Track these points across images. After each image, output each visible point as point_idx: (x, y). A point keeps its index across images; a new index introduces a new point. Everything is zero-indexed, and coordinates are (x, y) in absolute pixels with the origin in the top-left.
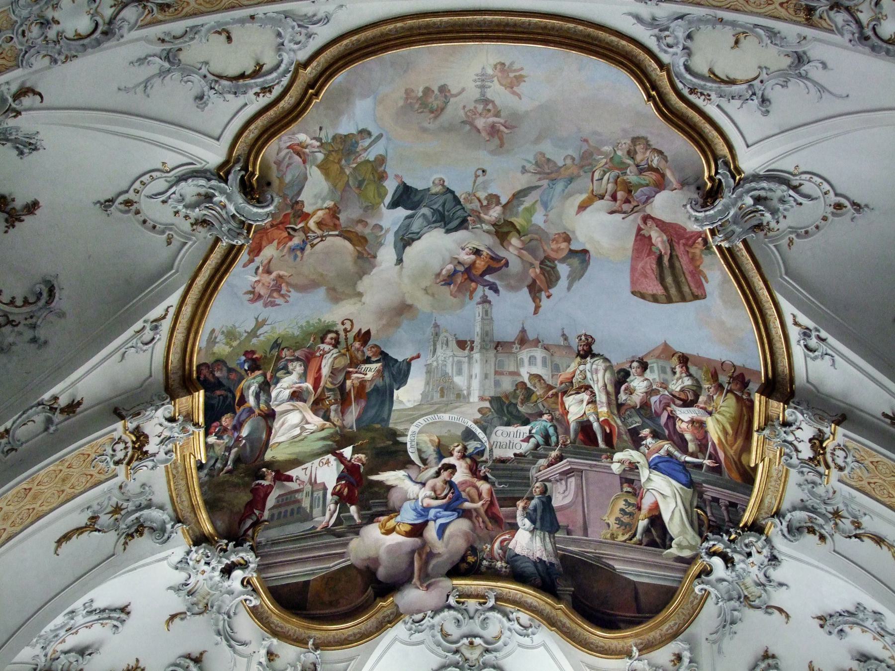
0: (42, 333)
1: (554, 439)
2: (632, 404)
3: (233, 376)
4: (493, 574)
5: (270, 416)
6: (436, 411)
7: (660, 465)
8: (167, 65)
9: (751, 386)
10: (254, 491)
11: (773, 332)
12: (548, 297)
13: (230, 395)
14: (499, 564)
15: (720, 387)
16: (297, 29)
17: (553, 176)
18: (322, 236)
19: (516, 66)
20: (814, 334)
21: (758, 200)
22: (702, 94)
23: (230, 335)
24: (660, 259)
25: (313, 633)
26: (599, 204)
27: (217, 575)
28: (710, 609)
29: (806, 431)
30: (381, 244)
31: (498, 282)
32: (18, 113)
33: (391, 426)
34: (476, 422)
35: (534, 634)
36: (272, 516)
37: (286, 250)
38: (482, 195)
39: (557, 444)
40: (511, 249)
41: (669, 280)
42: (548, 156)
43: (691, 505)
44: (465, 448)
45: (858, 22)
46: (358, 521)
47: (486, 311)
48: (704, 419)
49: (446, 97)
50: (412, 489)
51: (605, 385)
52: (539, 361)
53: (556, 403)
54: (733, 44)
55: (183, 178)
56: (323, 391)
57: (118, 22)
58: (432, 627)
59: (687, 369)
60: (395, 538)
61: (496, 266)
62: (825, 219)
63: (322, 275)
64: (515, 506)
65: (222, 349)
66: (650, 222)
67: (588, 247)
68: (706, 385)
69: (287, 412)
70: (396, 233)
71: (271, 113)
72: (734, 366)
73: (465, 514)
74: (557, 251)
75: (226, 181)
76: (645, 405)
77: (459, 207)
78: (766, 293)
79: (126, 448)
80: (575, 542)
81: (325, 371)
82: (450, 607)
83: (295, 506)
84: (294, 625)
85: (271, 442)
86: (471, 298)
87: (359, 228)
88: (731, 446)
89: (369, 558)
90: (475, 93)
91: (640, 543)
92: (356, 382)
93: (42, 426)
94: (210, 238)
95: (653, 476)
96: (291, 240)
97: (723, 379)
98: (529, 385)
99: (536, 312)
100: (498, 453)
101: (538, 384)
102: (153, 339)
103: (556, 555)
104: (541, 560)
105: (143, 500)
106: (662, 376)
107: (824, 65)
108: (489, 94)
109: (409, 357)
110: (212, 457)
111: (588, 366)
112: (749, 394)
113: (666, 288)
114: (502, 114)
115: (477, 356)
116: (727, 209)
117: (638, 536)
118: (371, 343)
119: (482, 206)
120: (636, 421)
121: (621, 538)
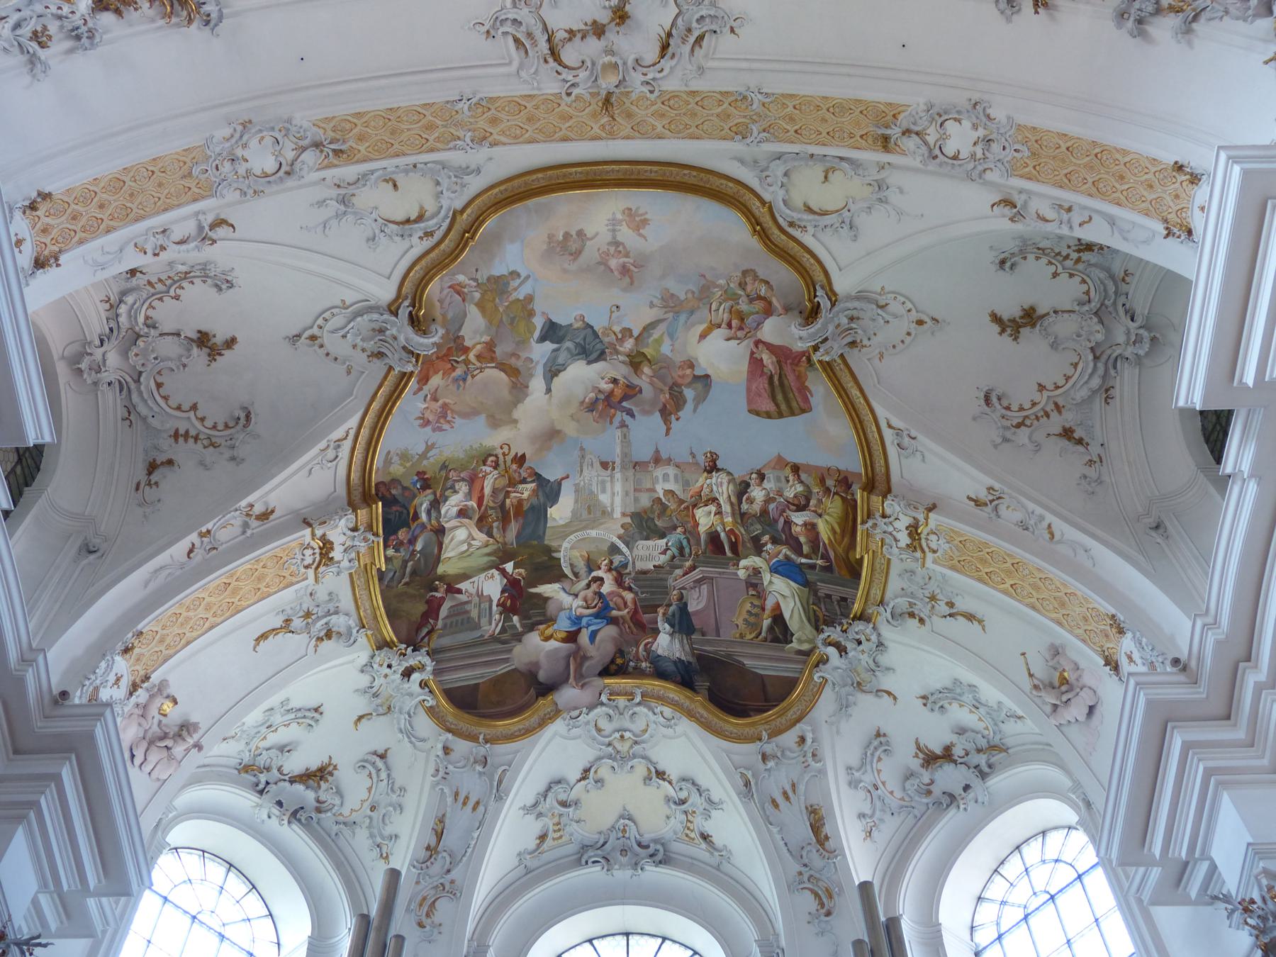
1: (687, 550)
2: (753, 513)
3: (406, 494)
4: (639, 673)
5: (440, 531)
6: (585, 528)
7: (780, 568)
8: (342, 208)
9: (853, 487)
10: (428, 602)
11: (870, 436)
12: (677, 419)
13: (405, 511)
14: (644, 665)
15: (827, 491)
16: (454, 179)
17: (677, 309)
18: (481, 368)
19: (641, 211)
20: (905, 433)
21: (852, 319)
22: (799, 227)
23: (404, 456)
24: (771, 378)
25: (483, 730)
26: (717, 332)
27: (398, 676)
28: (828, 694)
29: (905, 521)
30: (532, 376)
31: (634, 408)
32: (214, 241)
33: (546, 542)
34: (619, 537)
35: (676, 725)
36: (445, 626)
37: (450, 379)
38: (617, 329)
39: (690, 555)
40: (643, 377)
41: (780, 397)
42: (671, 292)
43: (808, 603)
44: (611, 562)
45: (926, 143)
46: (520, 629)
47: (625, 435)
48: (815, 521)
49: (583, 240)
50: (566, 600)
51: (729, 497)
52: (672, 478)
53: (688, 516)
54: (823, 179)
55: (359, 314)
56: (486, 509)
57: (297, 166)
58: (587, 723)
59: (799, 476)
60: (553, 644)
61: (631, 393)
62: (909, 334)
63: (482, 403)
64: (656, 612)
65: (397, 469)
66: (760, 346)
67: (709, 372)
68: (815, 490)
69: (456, 527)
70: (545, 365)
71: (433, 255)
72: (839, 470)
73: (614, 621)
74: (683, 377)
75: (396, 315)
76: (764, 512)
77: (598, 340)
78: (862, 400)
79: (314, 554)
80: (709, 642)
81: (487, 491)
82: (602, 704)
83: (465, 616)
84: (464, 721)
85: (443, 557)
86: (611, 423)
87: (513, 361)
88: (840, 545)
89: (531, 663)
90: (609, 239)
91: (765, 640)
92: (515, 501)
93: (240, 530)
94: (386, 369)
95: (774, 580)
96: (454, 371)
97: (830, 483)
98: (664, 500)
99: (667, 433)
100: (640, 565)
101: (671, 499)
102: (337, 457)
103: (693, 654)
104: (680, 659)
105: (331, 607)
106: (779, 485)
107: (901, 191)
108: (619, 238)
109: (559, 477)
110: (391, 570)
111: (714, 480)
112: (853, 495)
113: (777, 405)
114: (631, 255)
115: (618, 475)
116: (825, 326)
117: (763, 634)
118: (526, 465)
119: (617, 339)
120: (757, 529)
121: (749, 637)
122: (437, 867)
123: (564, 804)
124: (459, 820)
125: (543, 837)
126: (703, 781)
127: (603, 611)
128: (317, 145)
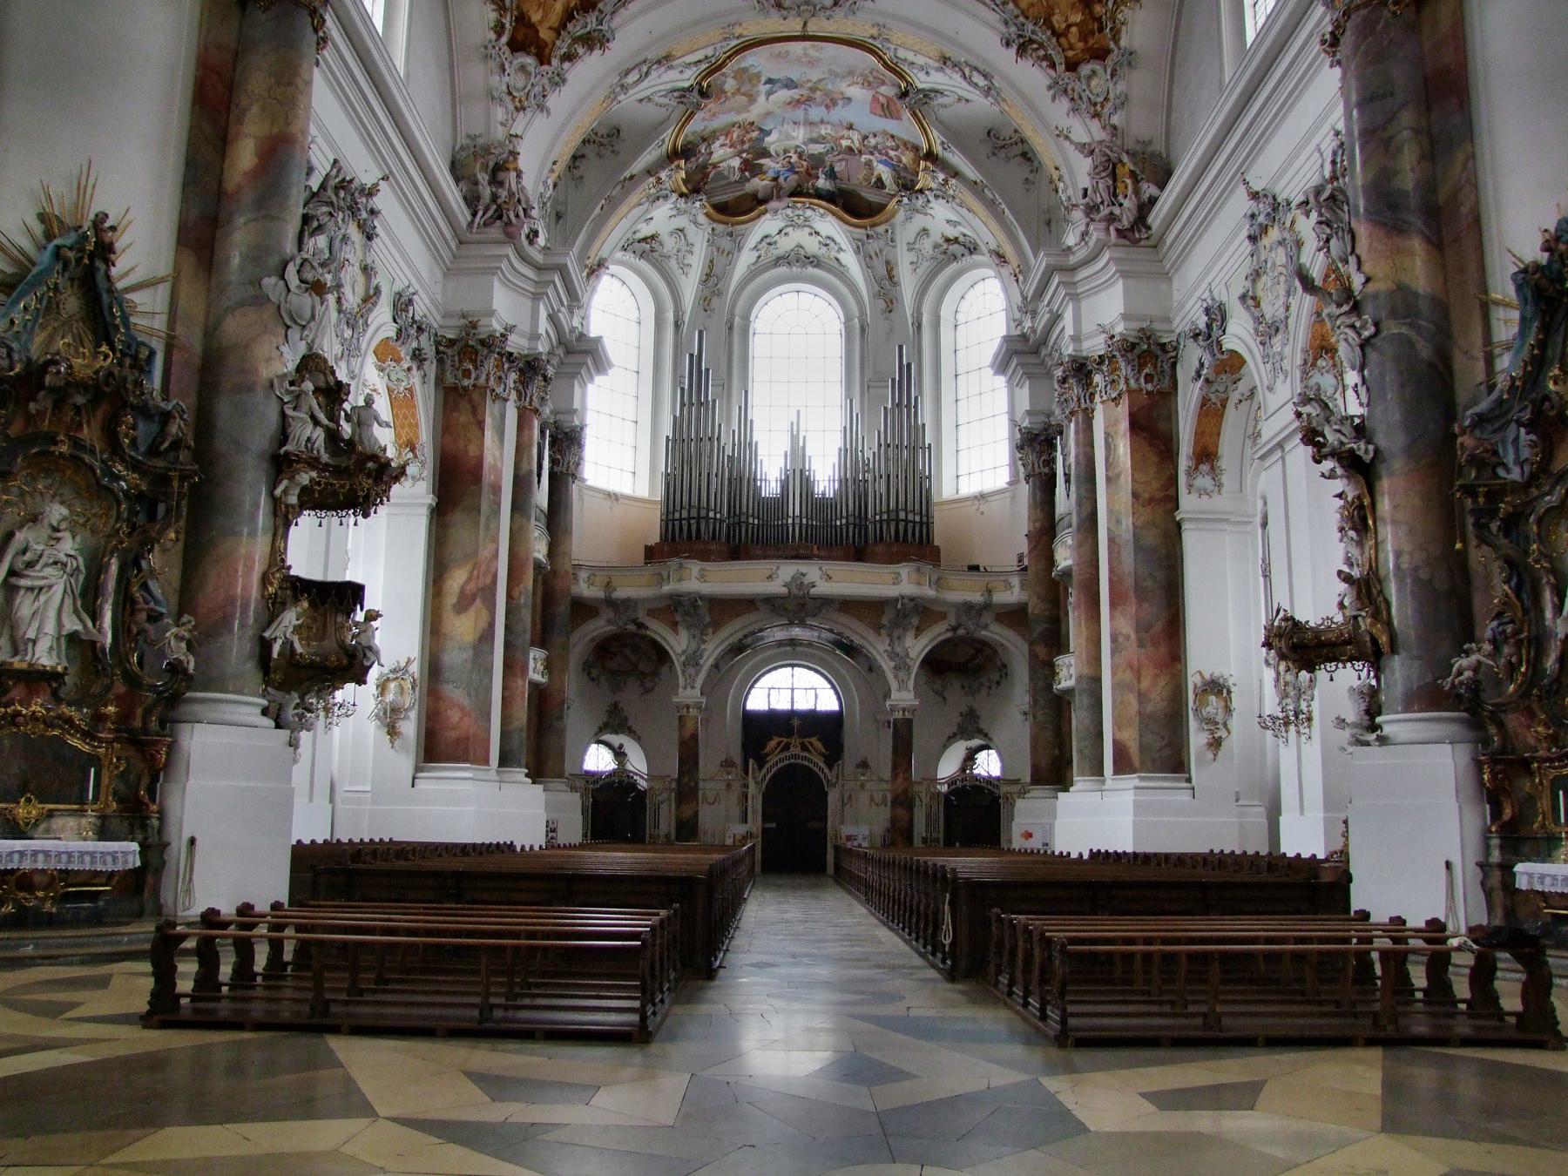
0: (616, 149)
4: (808, 195)
23: (694, 133)
28: (900, 216)
29: (941, 176)
50: (772, 165)
65: (691, 138)
73: (796, 173)
76: (875, 147)
81: (735, 136)
122: (710, 284)
123: (770, 244)
124: (720, 262)
125: (759, 257)
126: (838, 239)
127: (792, 169)
128: (659, 62)
